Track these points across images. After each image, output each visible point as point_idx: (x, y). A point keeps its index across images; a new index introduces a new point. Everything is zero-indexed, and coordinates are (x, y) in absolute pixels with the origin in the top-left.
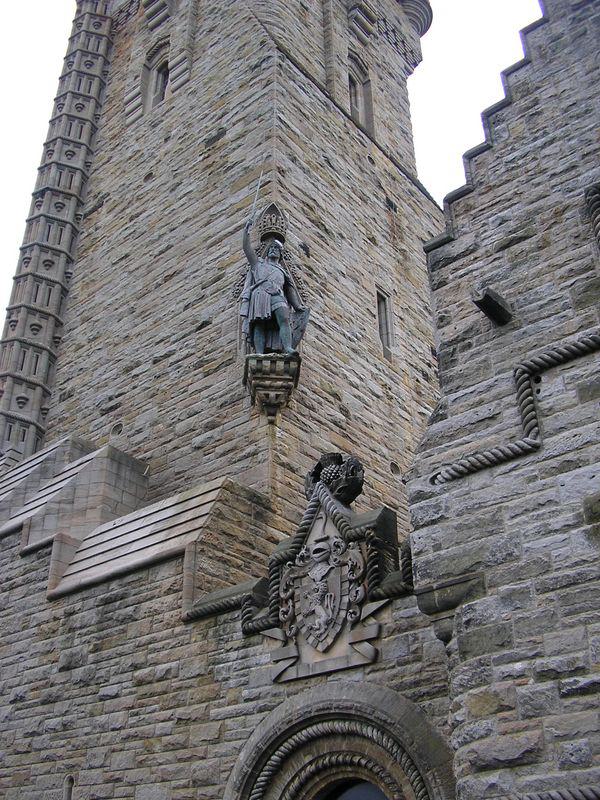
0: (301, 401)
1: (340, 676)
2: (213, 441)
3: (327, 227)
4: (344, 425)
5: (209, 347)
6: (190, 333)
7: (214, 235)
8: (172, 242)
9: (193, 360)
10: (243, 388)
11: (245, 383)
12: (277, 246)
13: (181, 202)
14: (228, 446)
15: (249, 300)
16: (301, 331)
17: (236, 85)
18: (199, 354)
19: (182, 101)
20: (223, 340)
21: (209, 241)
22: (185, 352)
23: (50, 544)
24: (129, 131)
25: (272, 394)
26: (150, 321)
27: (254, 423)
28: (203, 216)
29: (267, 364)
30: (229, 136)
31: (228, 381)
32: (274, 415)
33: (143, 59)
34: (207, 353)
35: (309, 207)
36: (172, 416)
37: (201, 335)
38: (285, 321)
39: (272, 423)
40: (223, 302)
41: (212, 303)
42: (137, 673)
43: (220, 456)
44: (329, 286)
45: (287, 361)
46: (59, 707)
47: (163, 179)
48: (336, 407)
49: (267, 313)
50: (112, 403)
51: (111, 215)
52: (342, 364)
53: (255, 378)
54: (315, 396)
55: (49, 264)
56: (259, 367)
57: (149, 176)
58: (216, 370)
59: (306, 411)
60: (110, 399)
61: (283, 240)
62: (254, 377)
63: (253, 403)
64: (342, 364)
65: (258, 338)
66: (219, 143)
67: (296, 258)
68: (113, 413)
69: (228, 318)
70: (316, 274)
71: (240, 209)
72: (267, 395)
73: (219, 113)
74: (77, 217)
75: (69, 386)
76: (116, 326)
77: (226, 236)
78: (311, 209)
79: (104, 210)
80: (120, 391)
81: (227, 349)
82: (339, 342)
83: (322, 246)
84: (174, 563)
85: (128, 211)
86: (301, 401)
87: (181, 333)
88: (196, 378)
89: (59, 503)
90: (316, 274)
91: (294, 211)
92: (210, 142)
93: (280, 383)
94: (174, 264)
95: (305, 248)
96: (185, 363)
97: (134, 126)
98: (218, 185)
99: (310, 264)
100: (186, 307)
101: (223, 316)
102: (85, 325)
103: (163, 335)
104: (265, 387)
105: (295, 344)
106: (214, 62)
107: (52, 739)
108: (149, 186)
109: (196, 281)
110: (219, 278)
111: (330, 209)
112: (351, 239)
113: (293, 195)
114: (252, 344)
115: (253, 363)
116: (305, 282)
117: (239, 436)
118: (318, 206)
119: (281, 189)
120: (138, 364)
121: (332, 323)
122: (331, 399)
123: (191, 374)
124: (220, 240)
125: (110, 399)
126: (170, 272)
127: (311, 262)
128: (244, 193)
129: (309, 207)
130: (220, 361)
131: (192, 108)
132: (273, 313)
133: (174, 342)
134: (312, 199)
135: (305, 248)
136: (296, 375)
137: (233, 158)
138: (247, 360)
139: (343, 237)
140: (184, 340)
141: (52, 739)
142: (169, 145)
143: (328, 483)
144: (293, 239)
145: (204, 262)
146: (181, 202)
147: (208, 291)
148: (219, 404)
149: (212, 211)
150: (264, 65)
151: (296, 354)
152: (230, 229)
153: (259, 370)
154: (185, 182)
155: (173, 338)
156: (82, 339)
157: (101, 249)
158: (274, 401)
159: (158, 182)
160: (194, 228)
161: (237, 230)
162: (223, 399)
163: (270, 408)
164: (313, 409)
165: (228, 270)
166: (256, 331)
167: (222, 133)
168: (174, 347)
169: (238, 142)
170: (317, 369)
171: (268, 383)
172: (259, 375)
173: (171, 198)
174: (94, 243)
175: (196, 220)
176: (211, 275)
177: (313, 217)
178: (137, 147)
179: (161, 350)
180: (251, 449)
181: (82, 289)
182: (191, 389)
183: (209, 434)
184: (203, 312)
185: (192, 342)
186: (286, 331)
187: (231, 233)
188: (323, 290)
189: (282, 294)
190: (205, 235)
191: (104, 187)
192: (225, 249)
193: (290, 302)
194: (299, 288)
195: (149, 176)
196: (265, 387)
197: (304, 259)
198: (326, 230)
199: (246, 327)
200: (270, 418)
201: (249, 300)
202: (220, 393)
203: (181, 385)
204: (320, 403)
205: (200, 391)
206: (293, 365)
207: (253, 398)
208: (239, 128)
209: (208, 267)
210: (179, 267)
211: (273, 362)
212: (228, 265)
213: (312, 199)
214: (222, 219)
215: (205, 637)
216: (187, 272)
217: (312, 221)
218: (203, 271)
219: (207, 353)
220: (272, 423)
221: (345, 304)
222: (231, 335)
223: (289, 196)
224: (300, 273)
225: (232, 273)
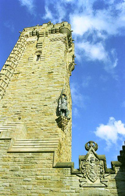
1: (99, 188)
8: (38, 87)
11: (56, 120)
14: (50, 131)
17: (56, 66)
19: (43, 63)
21: (48, 90)
22: (40, 109)
23: (10, 139)
24: (29, 63)
25: (64, 124)
26: (31, 100)
30: (54, 73)
33: (35, 52)
42: (37, 177)
46: (9, 180)
47: (37, 75)
50: (18, 113)
51: (22, 76)
55: (6, 79)
56: (63, 118)
57: (33, 73)
60: (18, 112)
66: (51, 74)
68: (18, 115)
72: (63, 124)
73: (52, 69)
74: (13, 73)
75: (5, 105)
76: (21, 98)
79: (20, 74)
80: (21, 111)
84: (50, 153)
85: (27, 77)
87: (39, 105)
89: (11, 130)
92: (49, 73)
93: (66, 123)
94: (38, 91)
97: (30, 62)
100: (41, 100)
101: (51, 105)
102: (12, 95)
103: (34, 104)
104: (63, 123)
106: (51, 60)
107: (5, 189)
108: (33, 74)
109: (44, 97)
110: (50, 98)
120: (27, 107)
125: (18, 112)
126: (38, 92)
131: (45, 65)
137: (55, 78)
141: (5, 189)
142: (38, 69)
143: (93, 147)
147: (47, 99)
150: (63, 65)
152: (54, 90)
155: (37, 105)
156: (12, 98)
157: (18, 82)
159: (35, 75)
165: (53, 97)
167: (53, 72)
168: (37, 107)
169: (57, 75)
173: (39, 79)
174: (17, 80)
178: (30, 66)
179: (33, 107)
180: (57, 133)
181: (12, 87)
182: (41, 117)
183: (45, 127)
184: (45, 103)
191: (21, 70)
195: (33, 73)
196: (63, 123)
208: (57, 73)
215: (59, 172)
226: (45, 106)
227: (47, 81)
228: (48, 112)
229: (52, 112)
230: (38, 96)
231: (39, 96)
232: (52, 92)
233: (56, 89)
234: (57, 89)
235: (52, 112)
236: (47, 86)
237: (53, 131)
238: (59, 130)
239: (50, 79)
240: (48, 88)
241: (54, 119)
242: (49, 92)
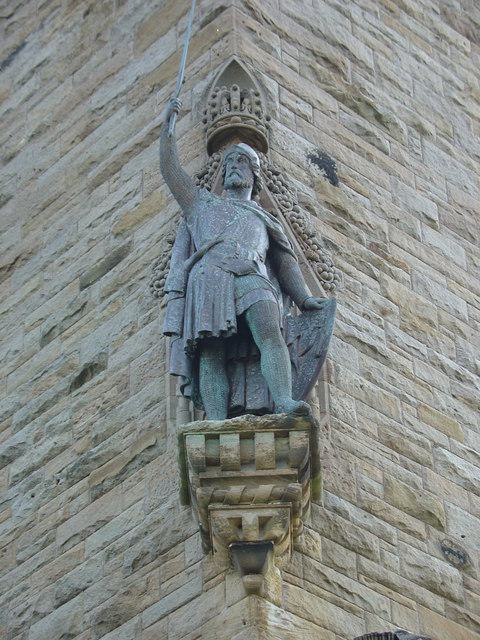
0: (334, 534)
3: (381, 110)
4: (456, 590)
5: (101, 425)
6: (57, 396)
7: (103, 156)
9: (66, 460)
10: (182, 511)
11: (187, 497)
12: (244, 158)
13: (25, 91)
15: (182, 293)
16: (311, 364)
18: (79, 446)
20: (133, 404)
22: (48, 444)
25: (250, 518)
27: (212, 598)
28: (75, 116)
29: (231, 441)
31: (148, 501)
32: (257, 570)
34: (96, 440)
35: (328, 63)
36: (22, 606)
37: (81, 398)
38: (269, 332)
39: (254, 591)
40: (130, 312)
41: (105, 319)
44: (395, 252)
45: (283, 432)
48: (431, 546)
49: (226, 321)
52: (444, 440)
53: (204, 482)
54: (372, 522)
56: (212, 452)
58: (119, 479)
59: (349, 559)
61: (260, 143)
62: (204, 480)
63: (208, 549)
64: (444, 440)
65: (212, 382)
67: (301, 184)
69: (137, 342)
70: (355, 222)
71: (160, 86)
72: (239, 524)
77: (129, 154)
78: (335, 67)
81: (142, 422)
82: (428, 385)
83: (369, 157)
86: (334, 534)
87: (35, 402)
88: (75, 503)
90: (355, 222)
91: (289, 75)
93: (265, 489)
95: (324, 162)
96: (50, 471)
98: (107, 37)
99: (339, 200)
100: (47, 338)
101: (132, 346)
104: (230, 503)
105: (303, 390)
109: (67, 273)
111: (388, 67)
112: (447, 135)
113: (284, 36)
114: (196, 398)
115: (196, 444)
116: (328, 243)
118: (354, 59)
119: (253, 23)
121: (403, 338)
122: (418, 526)
123: (63, 497)
124: (118, 166)
127: (343, 195)
128: (161, 50)
129: (328, 63)
130: (127, 455)
132: (241, 319)
133: (22, 425)
134: (334, 44)
135: (324, 162)
136: (309, 466)
138: (182, 439)
139: (423, 132)
140: (43, 416)
144: (291, 144)
145: (83, 224)
146: (25, 91)
148: (128, 561)
149: (95, 101)
151: (302, 412)
153: (212, 463)
154: (33, 40)
155: (17, 418)
158: (254, 536)
160: (57, 147)
161: (152, 135)
162: (138, 547)
163: (248, 556)
164: (363, 551)
165: (140, 235)
166: (205, 366)
168: (20, 436)
170: (370, 453)
171: (235, 490)
172: (214, 473)
175: (60, 127)
176: (99, 254)
177: (339, 87)
182: (64, 533)
185: (62, 419)
186: (276, 361)
188: (379, 260)
189: (263, 269)
190: (81, 159)
192: (130, 186)
193: (287, 291)
194: (312, 259)
196: (230, 503)
197: (320, 190)
198: (378, 117)
199: (178, 362)
200: (248, 579)
201: (182, 293)
202: (132, 534)
203: (40, 527)
204: (385, 537)
205: (83, 535)
206: (298, 439)
207: (206, 535)
209: (90, 234)
210: (27, 243)
211: (247, 436)
212: (138, 222)
213: (334, 44)
214: (118, 115)
216: (46, 254)
217: (342, 99)
218: (82, 246)
219: (96, 440)
220: (254, 591)
221: (435, 290)
222: (153, 389)
223: (275, 42)
224: (310, 222)
225: (147, 240)
226: (80, 380)
227: (76, 58)
228: (118, 442)
230: (19, 296)
231: (29, 287)
236: (81, 126)
238: (225, 613)
239: (95, 23)
240: (95, 146)
241: (177, 495)
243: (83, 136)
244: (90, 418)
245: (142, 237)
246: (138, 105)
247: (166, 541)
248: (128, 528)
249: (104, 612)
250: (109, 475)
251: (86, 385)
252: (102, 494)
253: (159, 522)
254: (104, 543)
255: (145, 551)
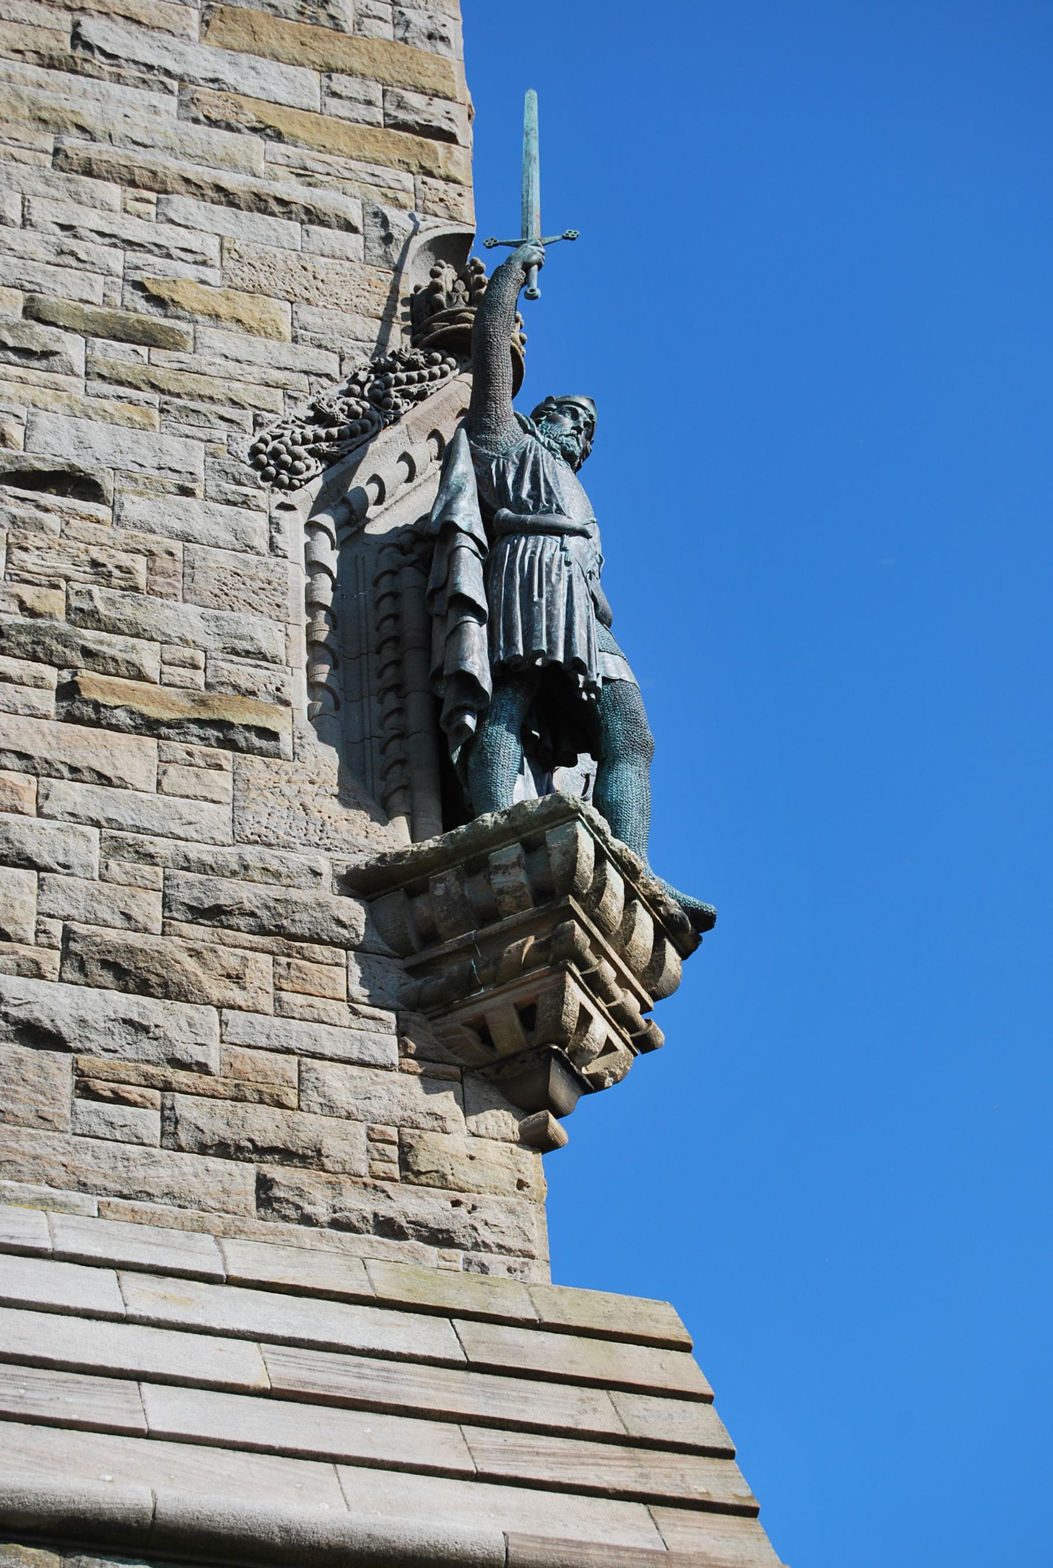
2: (150, 1049)
14: (264, 1124)
20: (181, 617)
25: (600, 1029)
34: (90, 618)
43: (203, 1149)
58: (150, 726)
104: (595, 985)
117: (330, 1108)
152: (230, 180)
162: (230, 891)
165: (214, 337)
187: (226, 197)
229: (244, 673)
232: (183, 205)
233: (254, 164)
234: (303, 174)
235: (244, 673)
237: (311, 1127)
242: (113, 192)
243: (50, 63)
244: (66, 567)
245: (219, 346)
246: (213, 123)
247: (302, 923)
248: (180, 831)
249: (131, 950)
250: (137, 707)
251: (49, 499)
252: (96, 724)
253: (277, 875)
254: (109, 820)
255: (247, 906)
